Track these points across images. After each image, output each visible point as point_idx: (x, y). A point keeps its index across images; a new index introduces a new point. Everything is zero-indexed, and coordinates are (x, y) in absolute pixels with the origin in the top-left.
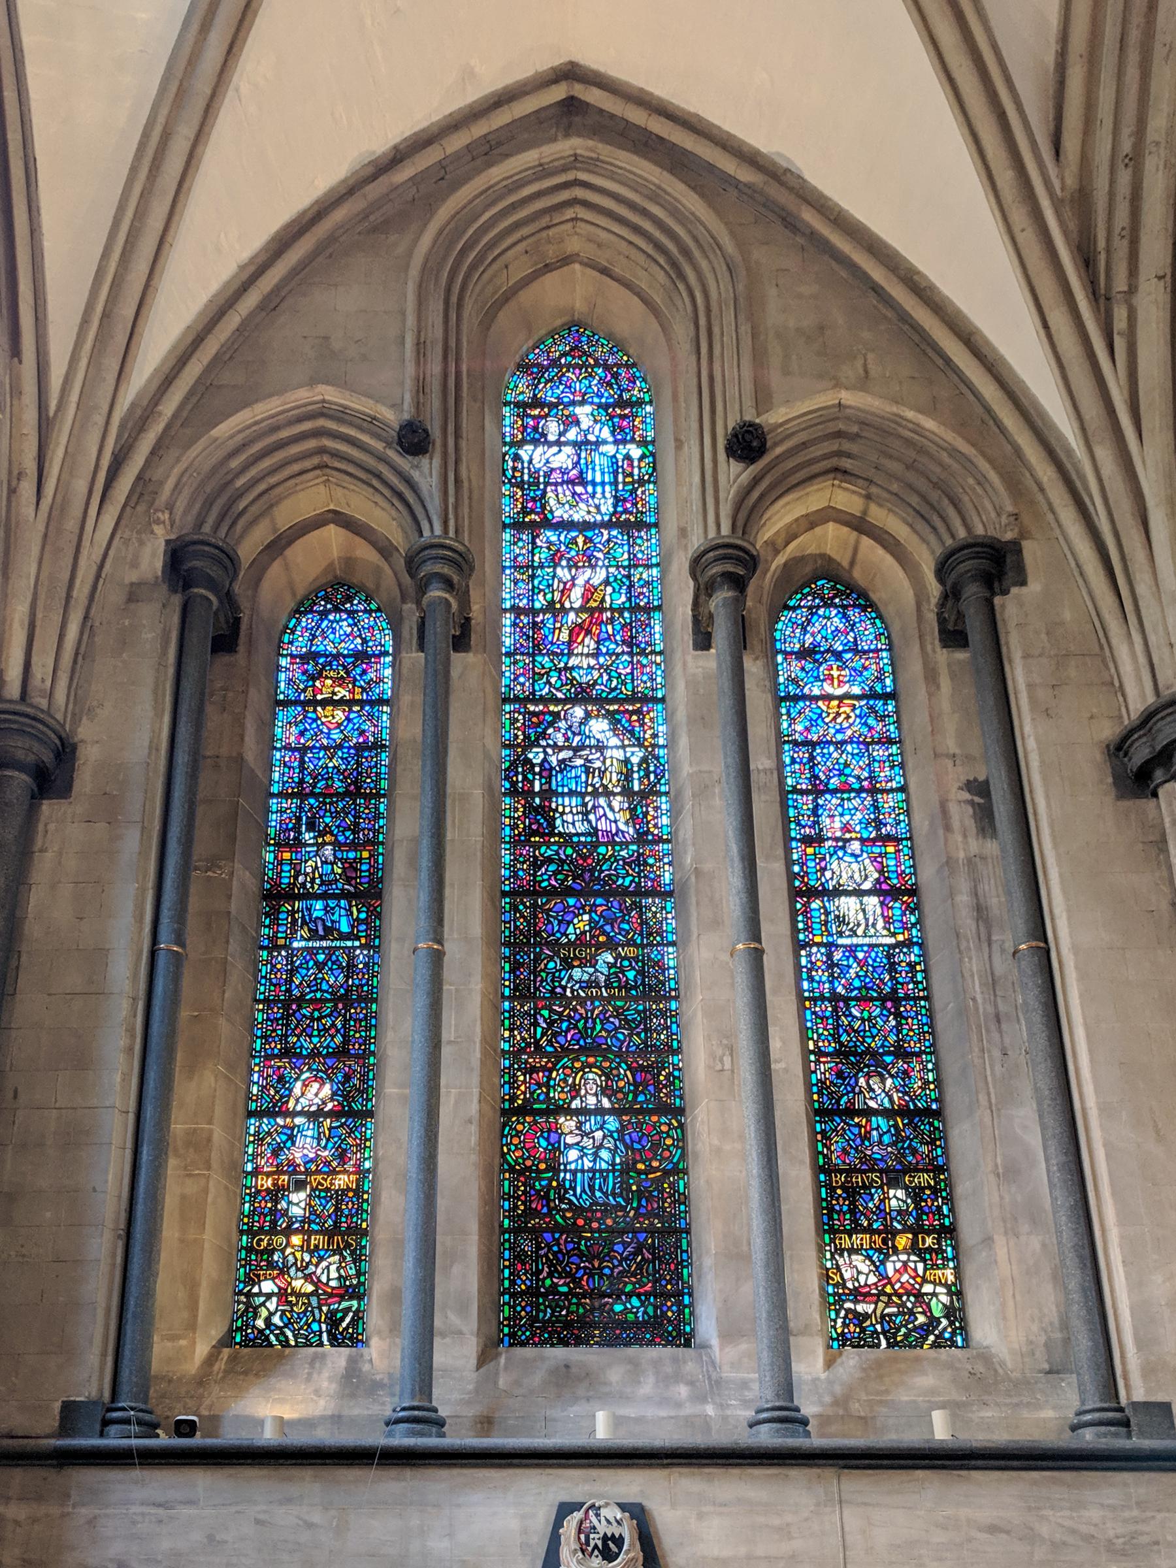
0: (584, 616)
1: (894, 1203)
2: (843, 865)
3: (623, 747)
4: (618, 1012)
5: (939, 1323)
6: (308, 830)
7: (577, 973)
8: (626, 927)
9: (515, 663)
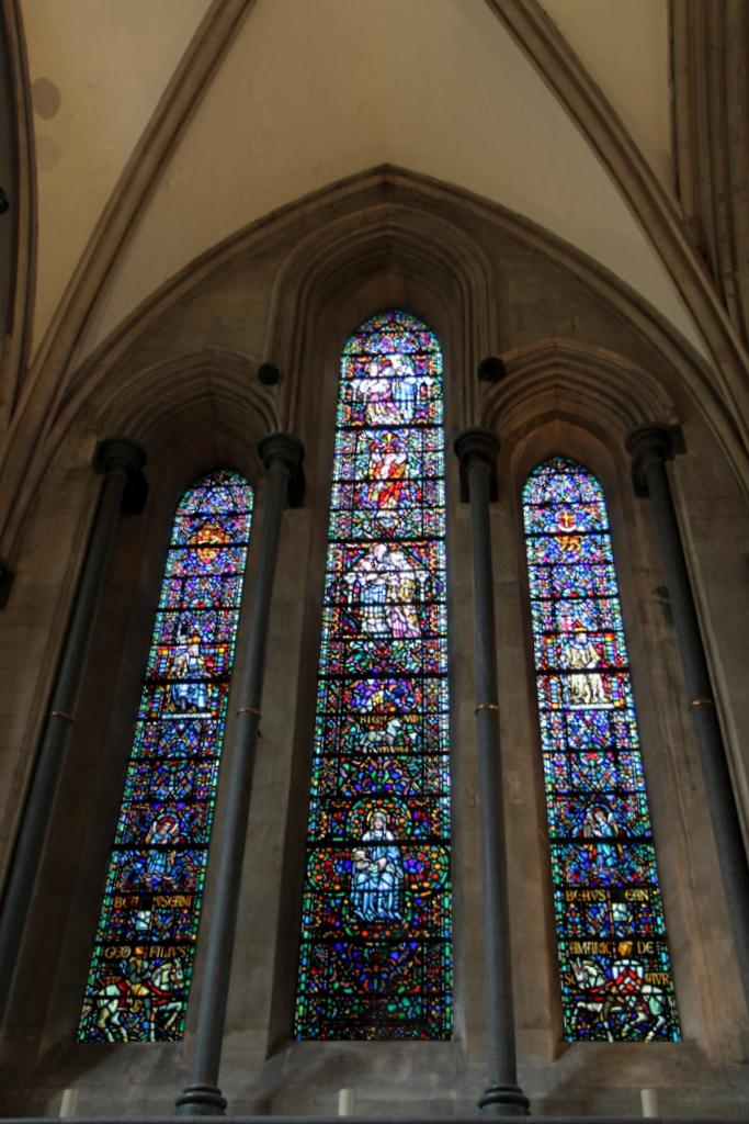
0: (390, 484)
1: (616, 915)
2: (574, 651)
3: (414, 571)
4: (403, 765)
5: (657, 1020)
6: (182, 634)
8: (410, 700)
9: (341, 515)
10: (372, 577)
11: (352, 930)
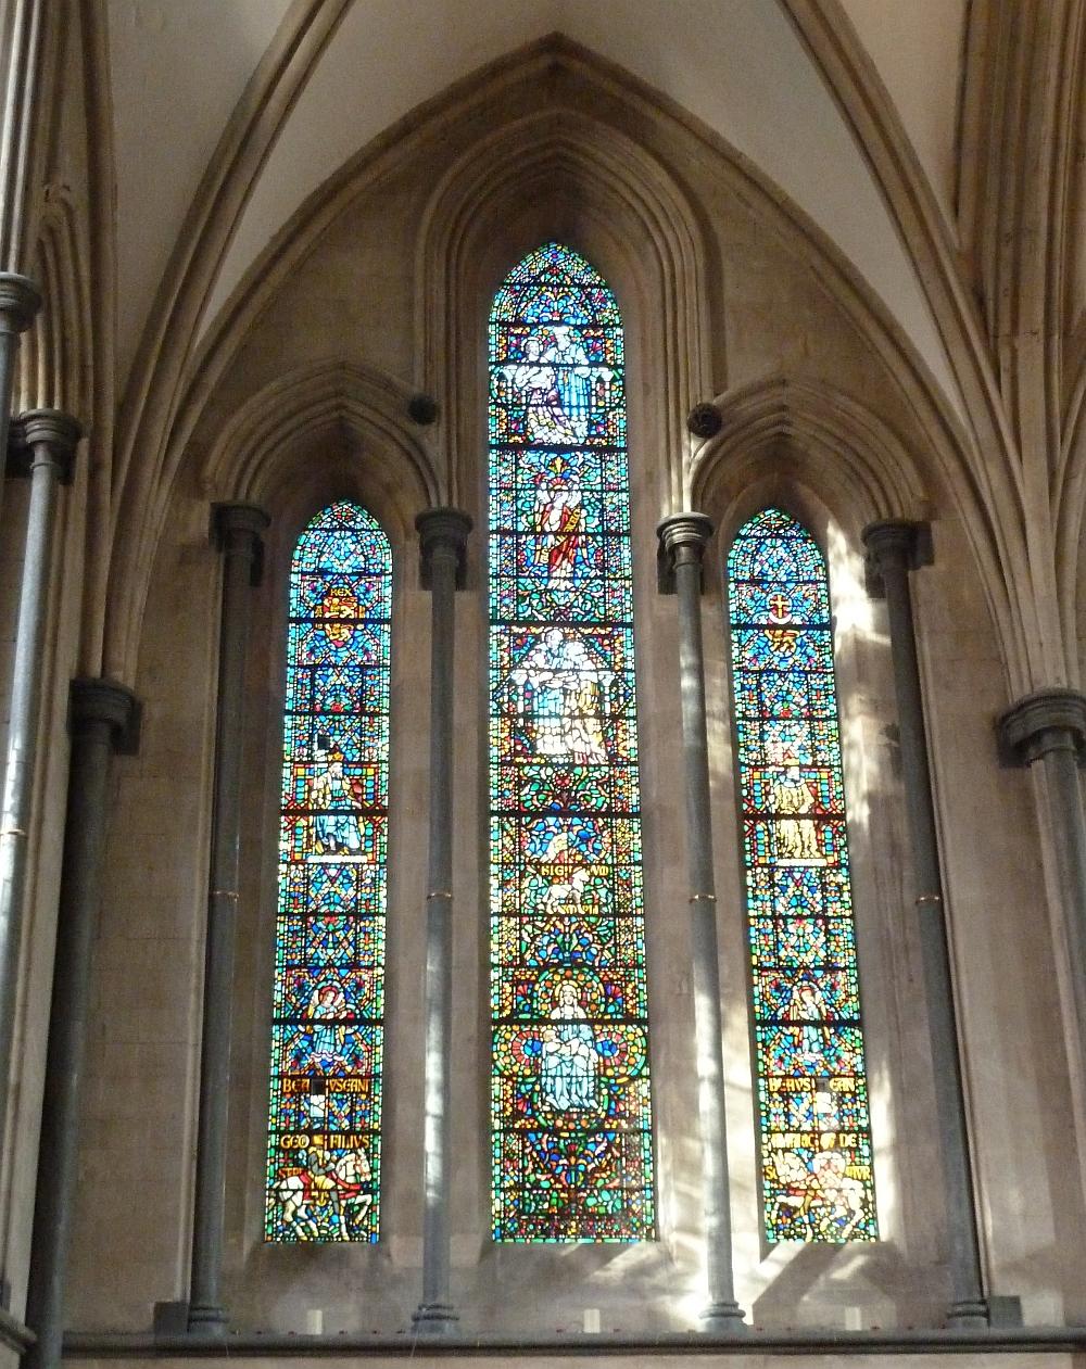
0: (562, 539)
4: (592, 928)
6: (319, 748)
8: (597, 846)
10: (547, 676)
11: (545, 1118)
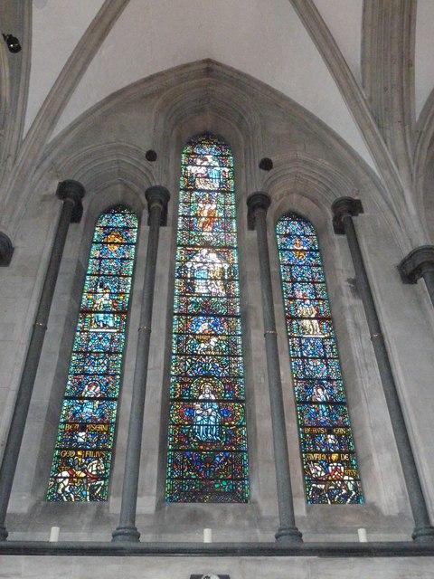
1: (330, 441)
3: (221, 263)
4: (219, 361)
7: (202, 345)
